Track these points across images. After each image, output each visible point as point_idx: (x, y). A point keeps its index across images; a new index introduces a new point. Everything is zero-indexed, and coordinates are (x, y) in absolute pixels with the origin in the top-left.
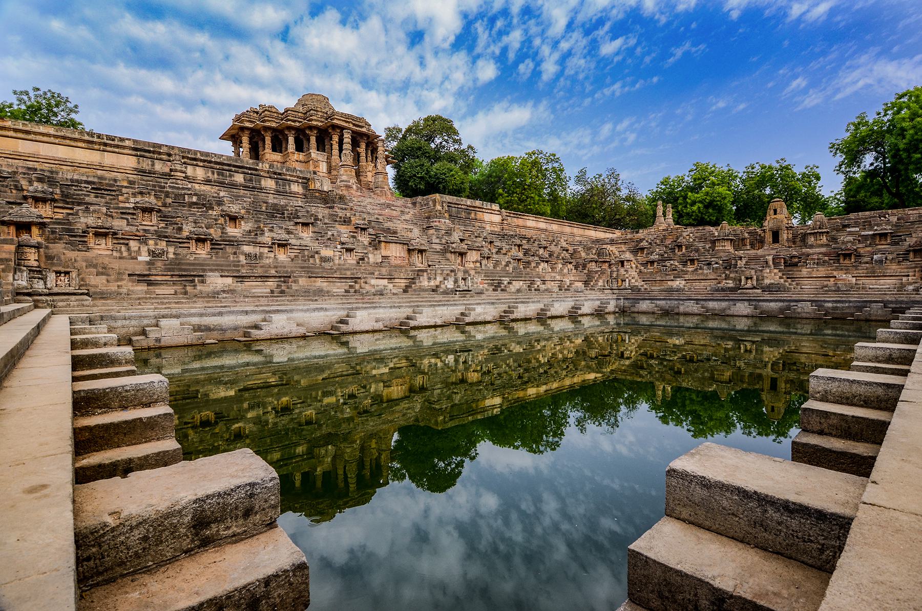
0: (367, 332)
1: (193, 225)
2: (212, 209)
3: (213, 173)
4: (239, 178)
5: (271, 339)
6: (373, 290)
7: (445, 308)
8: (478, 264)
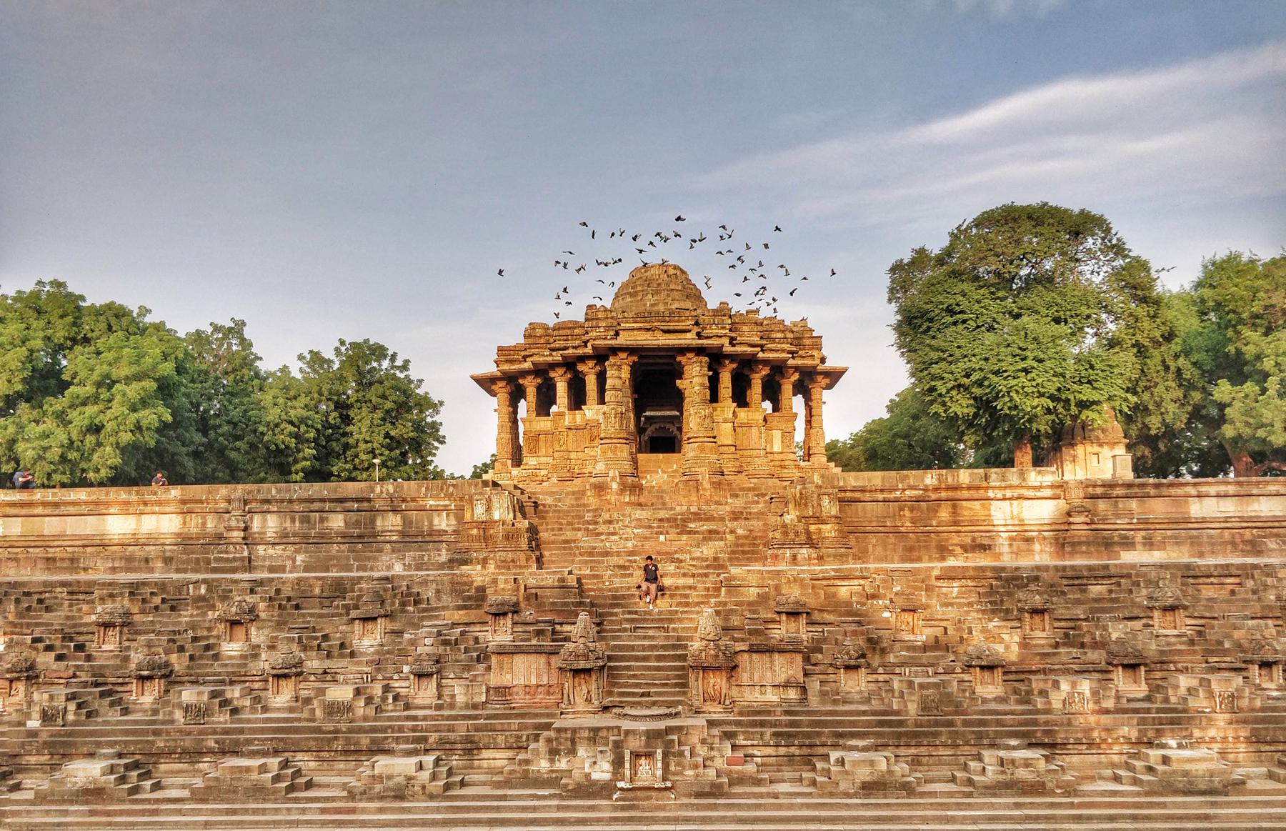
1: (145, 649)
2: (213, 607)
3: (293, 521)
4: (337, 522)
8: (793, 694)
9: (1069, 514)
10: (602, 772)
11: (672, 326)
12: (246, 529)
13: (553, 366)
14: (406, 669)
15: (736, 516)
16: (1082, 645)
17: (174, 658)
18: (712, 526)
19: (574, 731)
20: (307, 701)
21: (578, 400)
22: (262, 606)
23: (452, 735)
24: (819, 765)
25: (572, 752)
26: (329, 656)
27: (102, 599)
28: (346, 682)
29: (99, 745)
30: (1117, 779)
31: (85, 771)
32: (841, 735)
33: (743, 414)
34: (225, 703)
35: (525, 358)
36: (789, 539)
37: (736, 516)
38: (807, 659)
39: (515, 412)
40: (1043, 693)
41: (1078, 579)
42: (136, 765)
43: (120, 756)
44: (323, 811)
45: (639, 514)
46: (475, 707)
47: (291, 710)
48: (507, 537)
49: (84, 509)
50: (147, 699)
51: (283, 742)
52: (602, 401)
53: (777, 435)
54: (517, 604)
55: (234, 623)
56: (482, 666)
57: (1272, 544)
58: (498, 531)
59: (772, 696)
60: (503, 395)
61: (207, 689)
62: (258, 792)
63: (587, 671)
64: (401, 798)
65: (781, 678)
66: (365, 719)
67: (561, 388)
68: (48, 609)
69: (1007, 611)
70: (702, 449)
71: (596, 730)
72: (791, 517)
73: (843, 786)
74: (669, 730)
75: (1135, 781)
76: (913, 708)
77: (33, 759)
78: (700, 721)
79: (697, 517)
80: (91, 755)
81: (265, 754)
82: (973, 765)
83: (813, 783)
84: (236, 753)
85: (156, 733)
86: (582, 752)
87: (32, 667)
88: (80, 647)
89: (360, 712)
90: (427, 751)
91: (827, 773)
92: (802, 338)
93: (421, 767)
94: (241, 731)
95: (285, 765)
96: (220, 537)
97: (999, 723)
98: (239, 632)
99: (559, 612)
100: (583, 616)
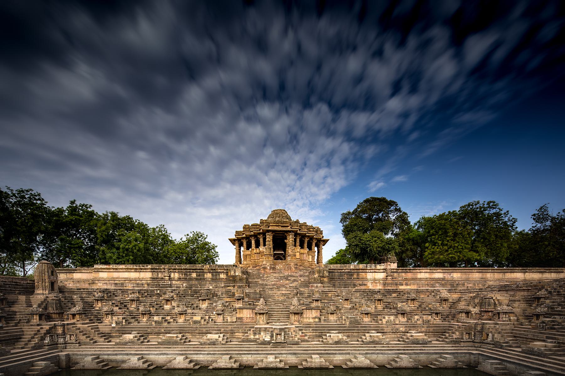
0: (183, 369)
4: (194, 275)
5: (130, 369)
6: (208, 342)
7: (250, 356)
8: (317, 320)
9: (387, 276)
10: (268, 338)
11: (284, 225)
12: (169, 276)
13: (251, 236)
14: (214, 313)
15: (301, 276)
16: (391, 308)
17: (151, 309)
18: (295, 278)
19: (260, 328)
20: (188, 320)
21: (257, 246)
22: (175, 296)
23: (227, 329)
24: (324, 337)
25: (260, 334)
26: (194, 309)
27: (131, 294)
28: (198, 316)
29: (132, 331)
30: (399, 341)
31: (129, 337)
32: (330, 330)
33: (302, 251)
34: (166, 320)
35: (243, 234)
36: (315, 281)
37: (301, 276)
38: (321, 312)
39: (240, 250)
40: (381, 320)
41: (389, 292)
42: (142, 336)
43: (138, 333)
44: (194, 348)
45: (275, 275)
46: (233, 322)
47: (184, 322)
48: (240, 280)
49: (124, 270)
50: (145, 319)
51: (182, 331)
52: (265, 245)
53: (310, 256)
54: (243, 297)
55: (168, 300)
56: (234, 312)
57: (437, 285)
58: (238, 278)
59: (311, 320)
60: (237, 245)
61: (161, 317)
62: (176, 343)
63: (263, 314)
64: (215, 345)
65: (314, 316)
66: (204, 325)
67: (253, 242)
68: (116, 296)
69: (372, 300)
70: (292, 258)
71: (266, 328)
72: (316, 276)
73: (331, 342)
74: (285, 328)
75: (404, 341)
76: (348, 323)
77: (114, 334)
78: (293, 326)
79: (291, 276)
80: (130, 333)
81: (177, 333)
82: (364, 337)
83: (323, 341)
84: (169, 333)
85: (148, 328)
86: (262, 333)
87: (112, 311)
88: (125, 306)
89: (203, 323)
90: (221, 333)
91: (326, 339)
92: (318, 231)
93: (219, 337)
94: (171, 327)
95: (183, 336)
96: (162, 278)
97: (370, 327)
98: (169, 303)
99: (255, 299)
100: (262, 299)
